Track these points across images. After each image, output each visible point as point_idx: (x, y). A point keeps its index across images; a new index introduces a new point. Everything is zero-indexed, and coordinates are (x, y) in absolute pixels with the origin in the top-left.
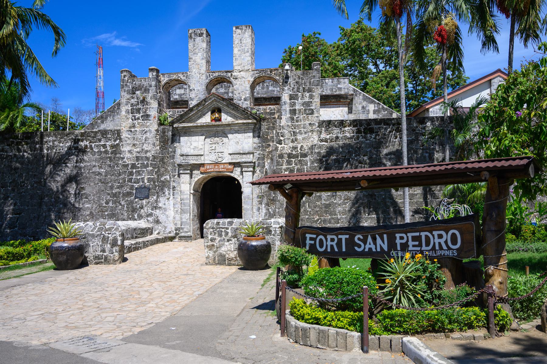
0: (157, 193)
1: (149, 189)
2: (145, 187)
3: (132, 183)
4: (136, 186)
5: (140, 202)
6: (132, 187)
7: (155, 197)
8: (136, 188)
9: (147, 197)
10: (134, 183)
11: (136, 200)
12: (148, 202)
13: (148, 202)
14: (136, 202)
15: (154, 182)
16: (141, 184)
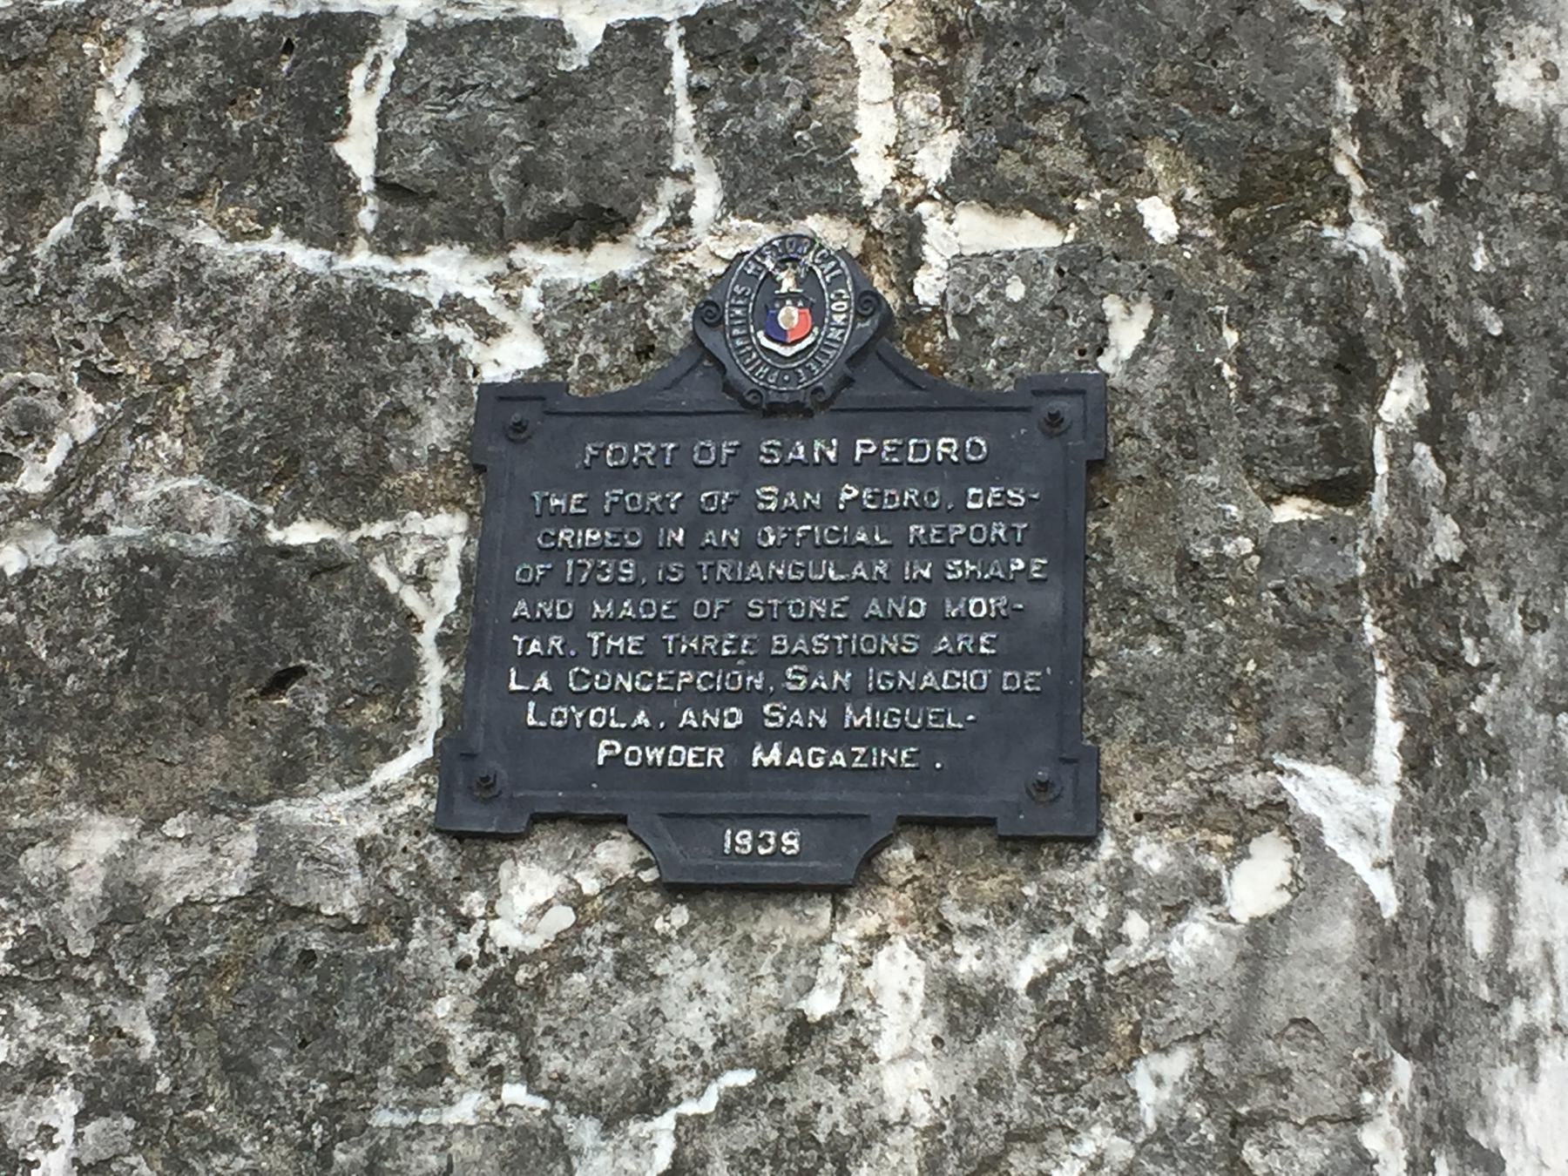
0: (1429, 613)
1: (1063, 440)
2: (887, 370)
3: (322, 208)
4: (498, 308)
5: (702, 988)
6: (326, 406)
7: (1353, 804)
8: (515, 420)
9: (1008, 791)
10: (421, 206)
11: (529, 898)
12: (1089, 1024)
13: (1089, 1024)
14: (504, 997)
15: (1267, 191)
16: (720, 238)
